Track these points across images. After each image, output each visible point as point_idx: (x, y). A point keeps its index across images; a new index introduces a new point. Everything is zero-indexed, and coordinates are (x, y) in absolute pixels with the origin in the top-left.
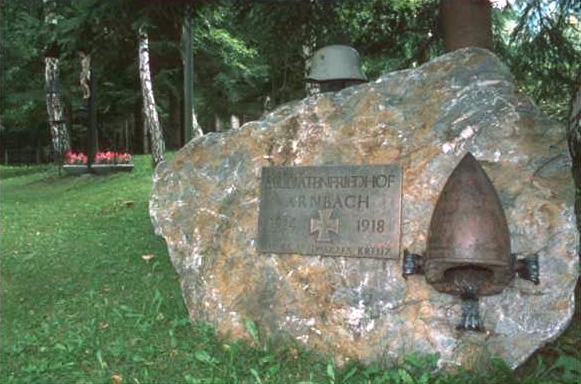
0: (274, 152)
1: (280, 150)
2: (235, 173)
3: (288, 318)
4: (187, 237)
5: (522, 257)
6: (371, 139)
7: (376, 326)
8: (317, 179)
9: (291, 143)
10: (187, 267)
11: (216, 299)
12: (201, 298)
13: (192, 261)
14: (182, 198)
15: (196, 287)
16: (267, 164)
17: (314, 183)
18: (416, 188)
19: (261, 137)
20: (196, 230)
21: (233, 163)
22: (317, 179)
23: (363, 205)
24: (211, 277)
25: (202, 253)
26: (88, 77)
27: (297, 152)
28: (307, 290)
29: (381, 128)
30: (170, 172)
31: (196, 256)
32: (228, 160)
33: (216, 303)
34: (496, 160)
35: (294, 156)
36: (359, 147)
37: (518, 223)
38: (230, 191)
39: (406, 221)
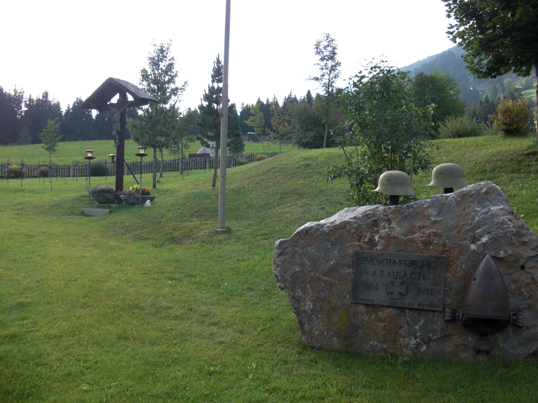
0: (362, 241)
1: (366, 240)
2: (336, 252)
3: (371, 343)
4: (302, 290)
5: (484, 190)
6: (426, 238)
7: (426, 348)
8: (392, 261)
9: (374, 236)
10: (302, 310)
11: (322, 329)
12: (312, 328)
13: (305, 305)
14: (298, 265)
15: (308, 322)
16: (358, 249)
17: (390, 263)
18: (454, 270)
19: (353, 230)
20: (308, 286)
21: (333, 244)
22: (392, 261)
23: (421, 278)
24: (319, 316)
25: (312, 301)
26: (119, 129)
27: (378, 241)
28: (384, 326)
29: (433, 232)
30: (287, 247)
31: (308, 303)
32: (330, 243)
33: (323, 332)
34: (501, 256)
35: (376, 245)
36: (419, 242)
37: (186, 394)
38: (332, 263)
39: (447, 288)
